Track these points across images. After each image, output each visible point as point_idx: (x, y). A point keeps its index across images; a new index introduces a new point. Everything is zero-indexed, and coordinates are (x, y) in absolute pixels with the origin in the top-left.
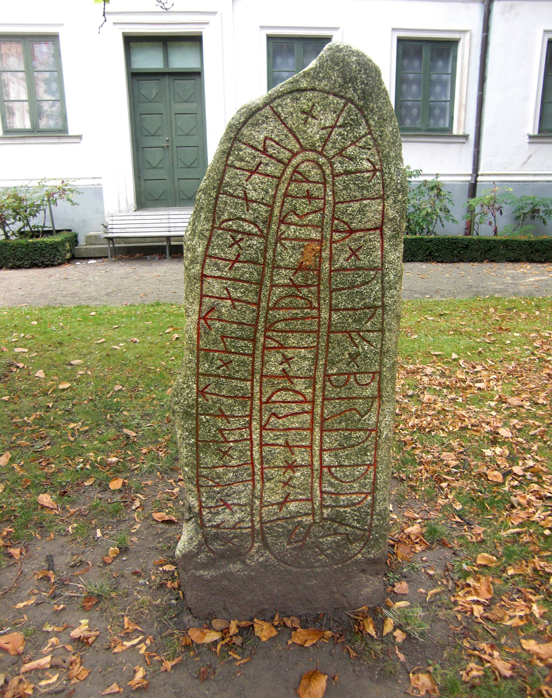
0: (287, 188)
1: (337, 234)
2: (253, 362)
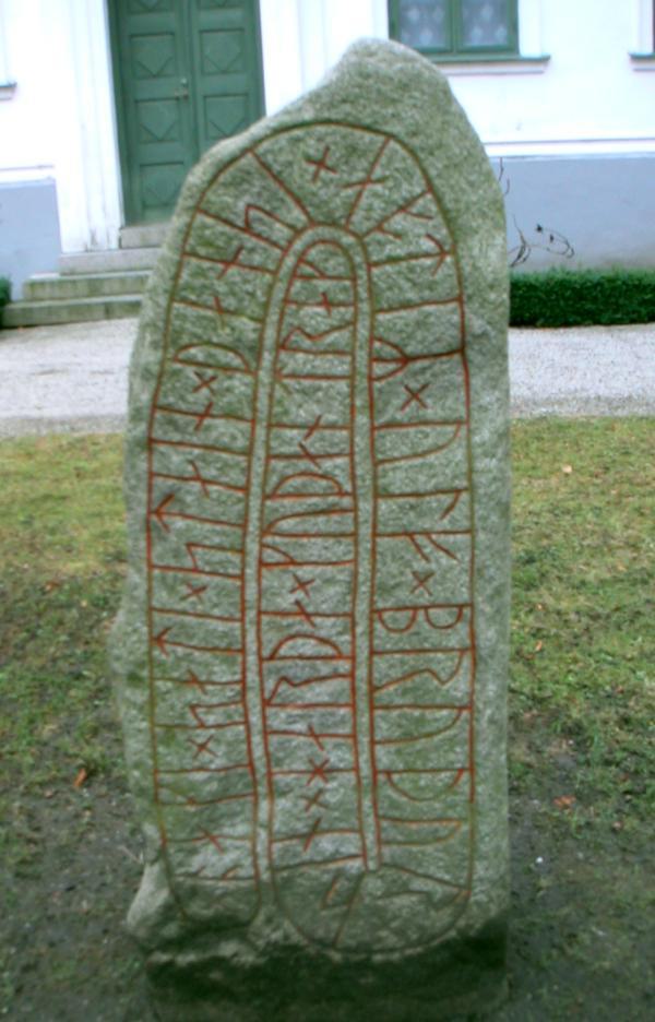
0: (288, 290)
2: (243, 588)
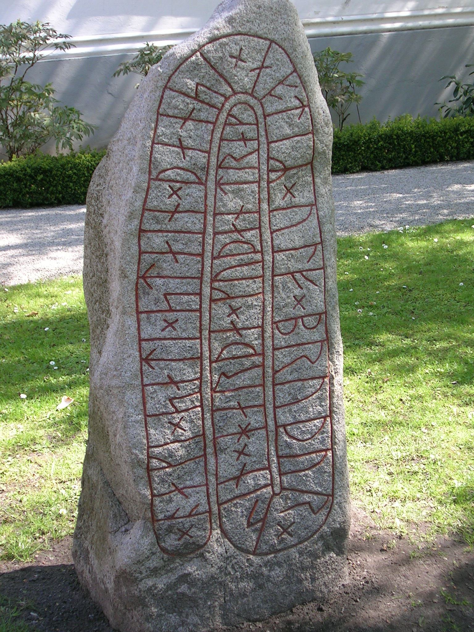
0: (222, 133)
1: (273, 173)
